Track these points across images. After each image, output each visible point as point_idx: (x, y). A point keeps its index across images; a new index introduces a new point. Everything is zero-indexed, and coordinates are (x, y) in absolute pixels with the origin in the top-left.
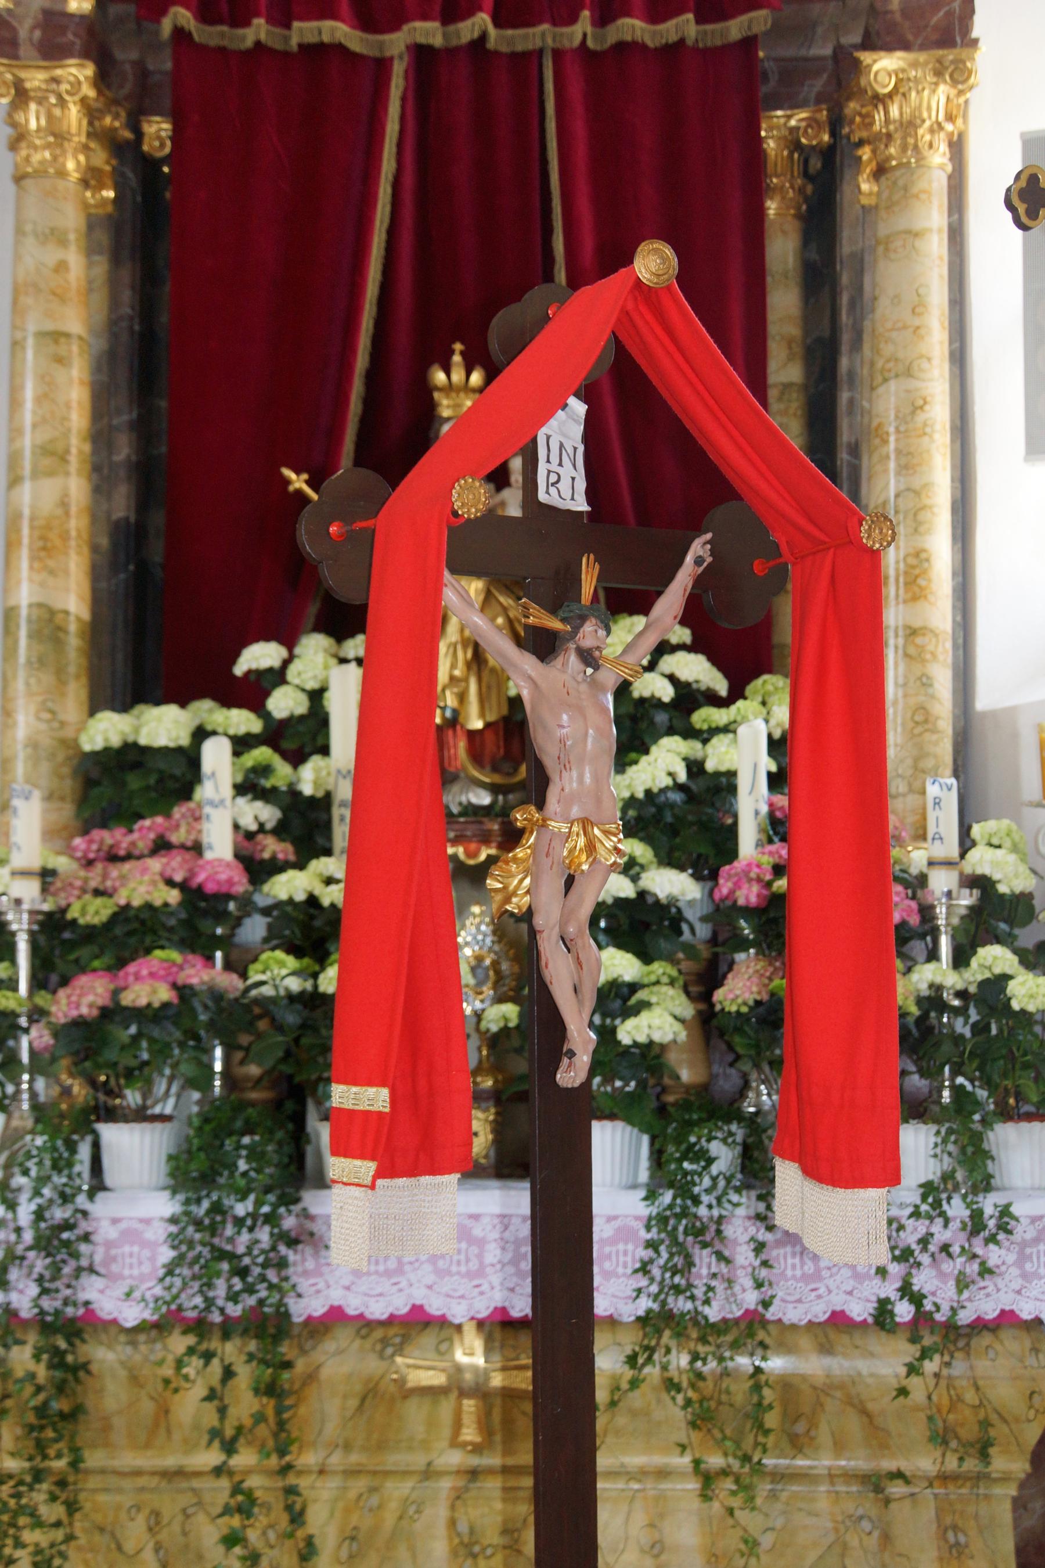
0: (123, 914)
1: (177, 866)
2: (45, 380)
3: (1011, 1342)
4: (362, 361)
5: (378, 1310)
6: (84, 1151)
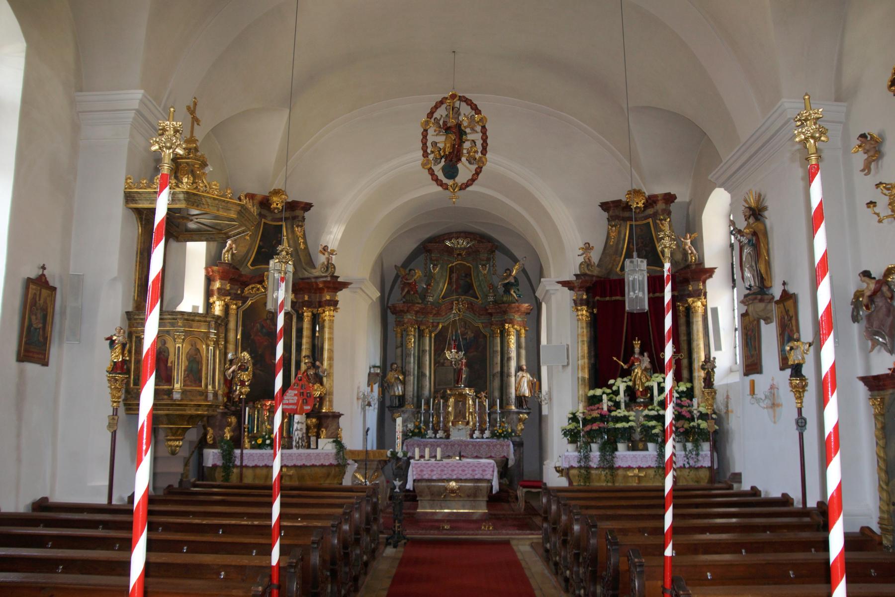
0: (593, 418)
1: (599, 411)
2: (582, 347)
3: (704, 470)
4: (624, 340)
5: (625, 466)
6: (589, 447)
